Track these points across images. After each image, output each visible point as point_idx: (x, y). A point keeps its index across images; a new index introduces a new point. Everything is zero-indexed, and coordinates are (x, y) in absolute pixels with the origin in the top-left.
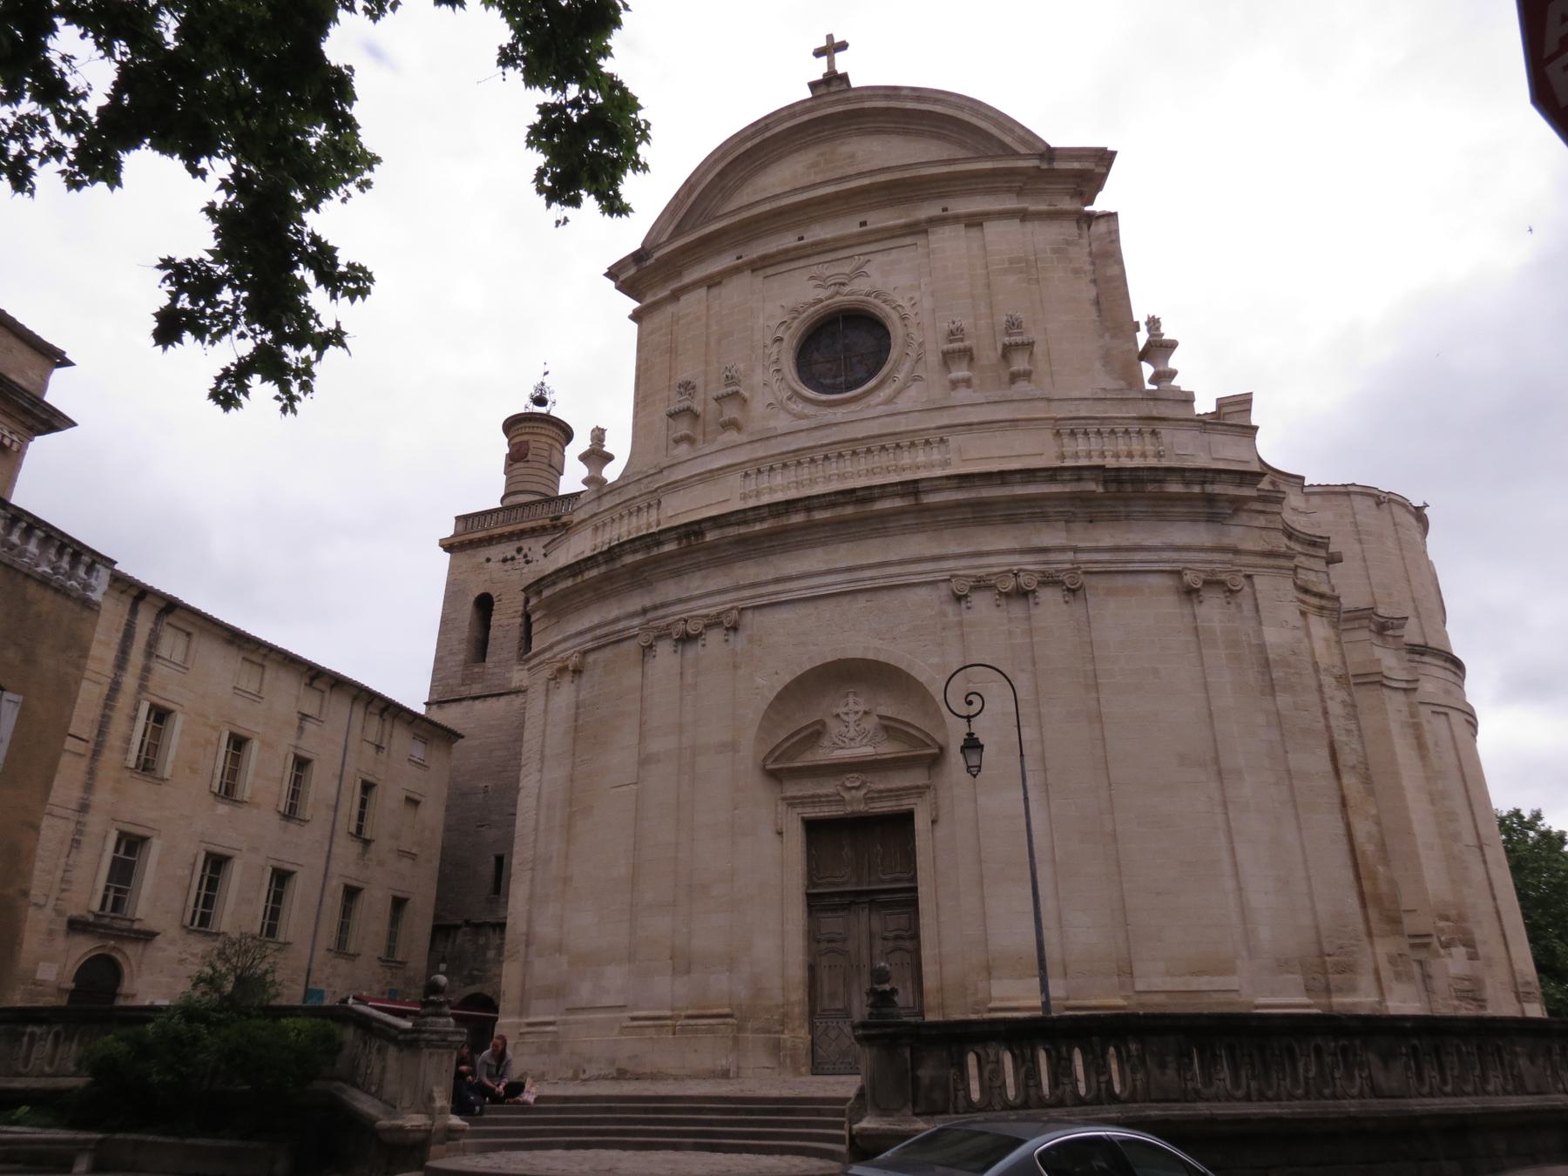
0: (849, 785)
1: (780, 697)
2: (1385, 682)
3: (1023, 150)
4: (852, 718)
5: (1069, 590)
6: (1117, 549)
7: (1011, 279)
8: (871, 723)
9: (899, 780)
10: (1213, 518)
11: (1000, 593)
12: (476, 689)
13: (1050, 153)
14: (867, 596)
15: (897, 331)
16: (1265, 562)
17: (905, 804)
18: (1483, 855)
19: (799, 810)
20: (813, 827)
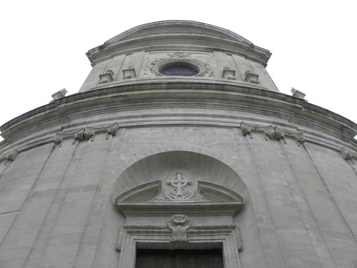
0: (176, 221)
1: (134, 166)
4: (179, 185)
9: (212, 222)
11: (267, 135)
14: (194, 128)
17: (216, 239)
19: (136, 237)
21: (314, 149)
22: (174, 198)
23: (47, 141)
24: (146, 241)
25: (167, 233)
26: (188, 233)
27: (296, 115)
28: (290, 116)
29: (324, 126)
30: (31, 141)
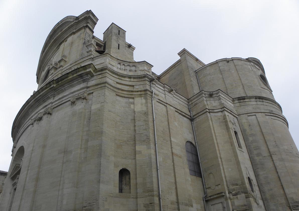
2: (210, 111)
3: (72, 20)
6: (60, 99)
10: (84, 81)
13: (77, 18)
16: (96, 87)
18: (272, 158)
27: (56, 90)
28: (53, 94)
29: (70, 84)
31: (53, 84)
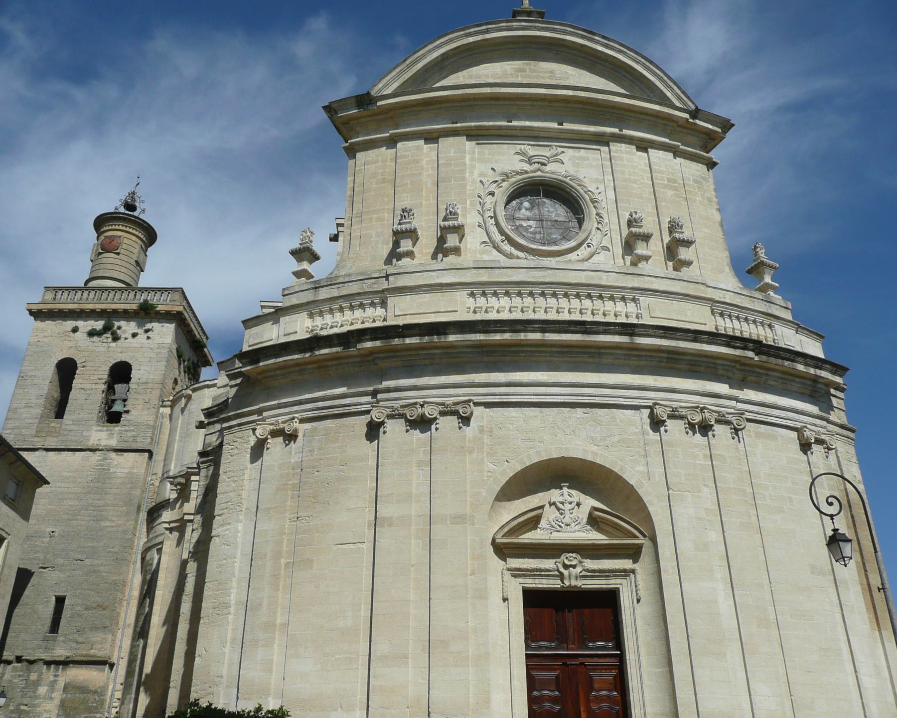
5: (735, 429)
7: (670, 193)
8: (583, 514)
11: (689, 423)
12: (51, 443)
15: (591, 212)
19: (521, 580)
20: (532, 598)
21: (758, 435)
22: (560, 526)
23: (353, 409)
24: (534, 586)
25: (557, 576)
26: (581, 577)
30: (321, 404)
31: (753, 350)
